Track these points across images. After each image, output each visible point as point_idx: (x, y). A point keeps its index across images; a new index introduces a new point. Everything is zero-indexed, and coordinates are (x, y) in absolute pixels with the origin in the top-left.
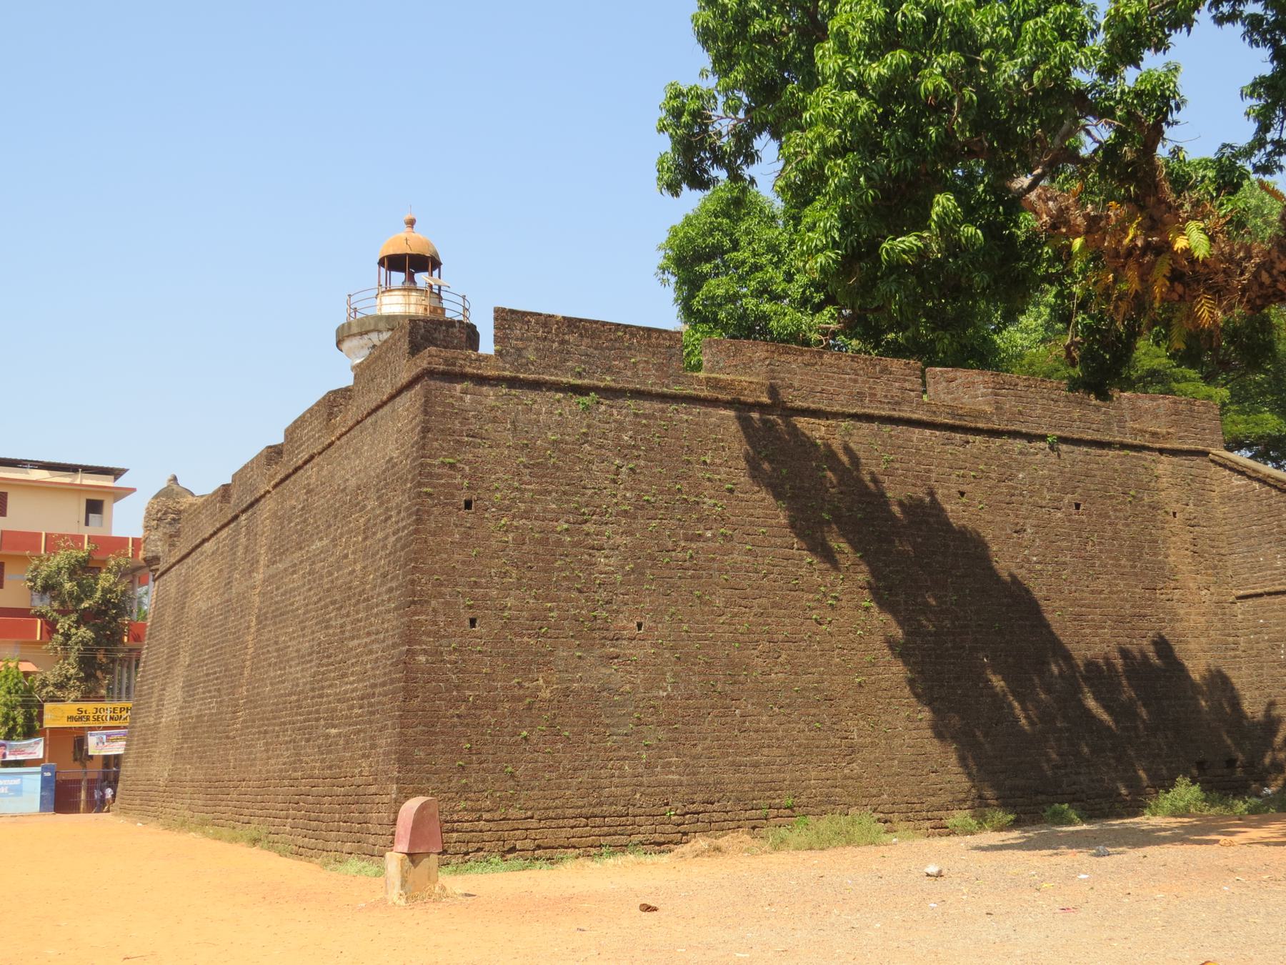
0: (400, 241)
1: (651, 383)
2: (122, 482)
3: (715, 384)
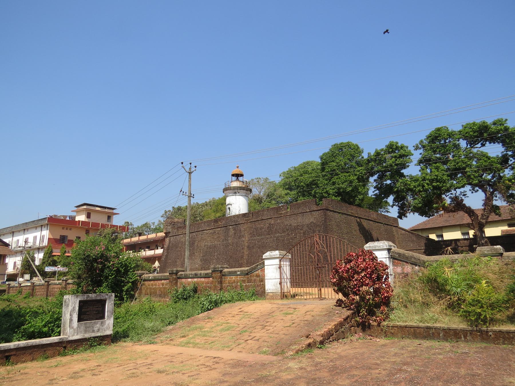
0: (236, 171)
1: (346, 212)
2: (115, 211)
3: (352, 213)
